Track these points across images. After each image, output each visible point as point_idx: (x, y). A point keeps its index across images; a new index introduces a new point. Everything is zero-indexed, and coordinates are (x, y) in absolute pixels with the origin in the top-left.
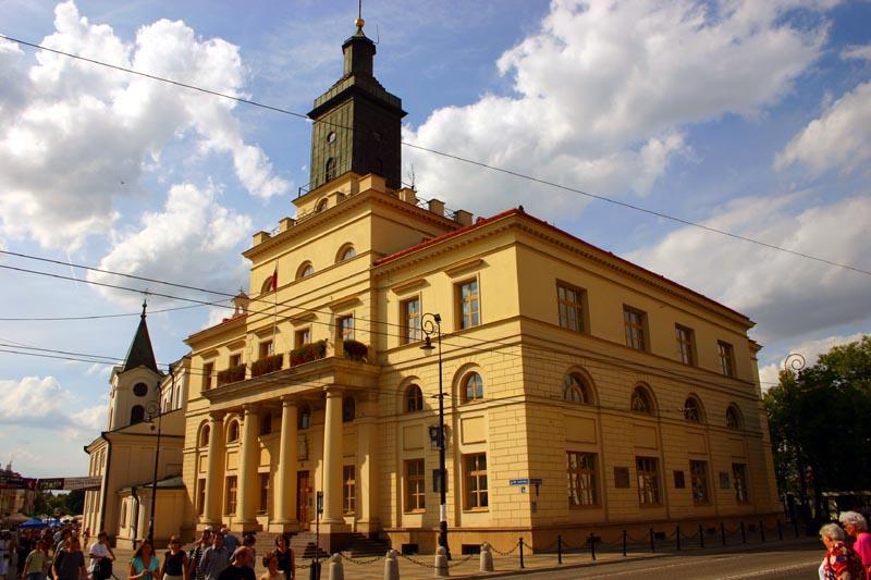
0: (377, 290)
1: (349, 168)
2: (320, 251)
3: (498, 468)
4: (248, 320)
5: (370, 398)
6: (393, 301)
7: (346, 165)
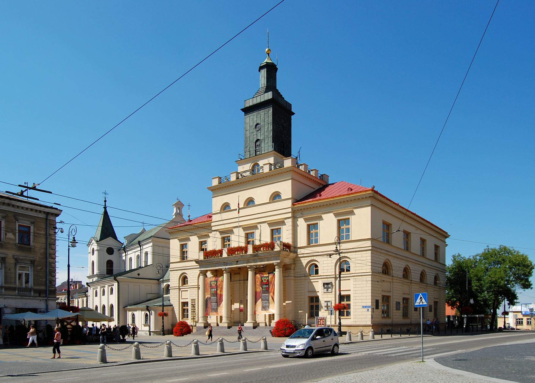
0: (294, 218)
1: (271, 149)
2: (261, 193)
3: (355, 301)
5: (292, 268)
6: (302, 224)
7: (268, 145)
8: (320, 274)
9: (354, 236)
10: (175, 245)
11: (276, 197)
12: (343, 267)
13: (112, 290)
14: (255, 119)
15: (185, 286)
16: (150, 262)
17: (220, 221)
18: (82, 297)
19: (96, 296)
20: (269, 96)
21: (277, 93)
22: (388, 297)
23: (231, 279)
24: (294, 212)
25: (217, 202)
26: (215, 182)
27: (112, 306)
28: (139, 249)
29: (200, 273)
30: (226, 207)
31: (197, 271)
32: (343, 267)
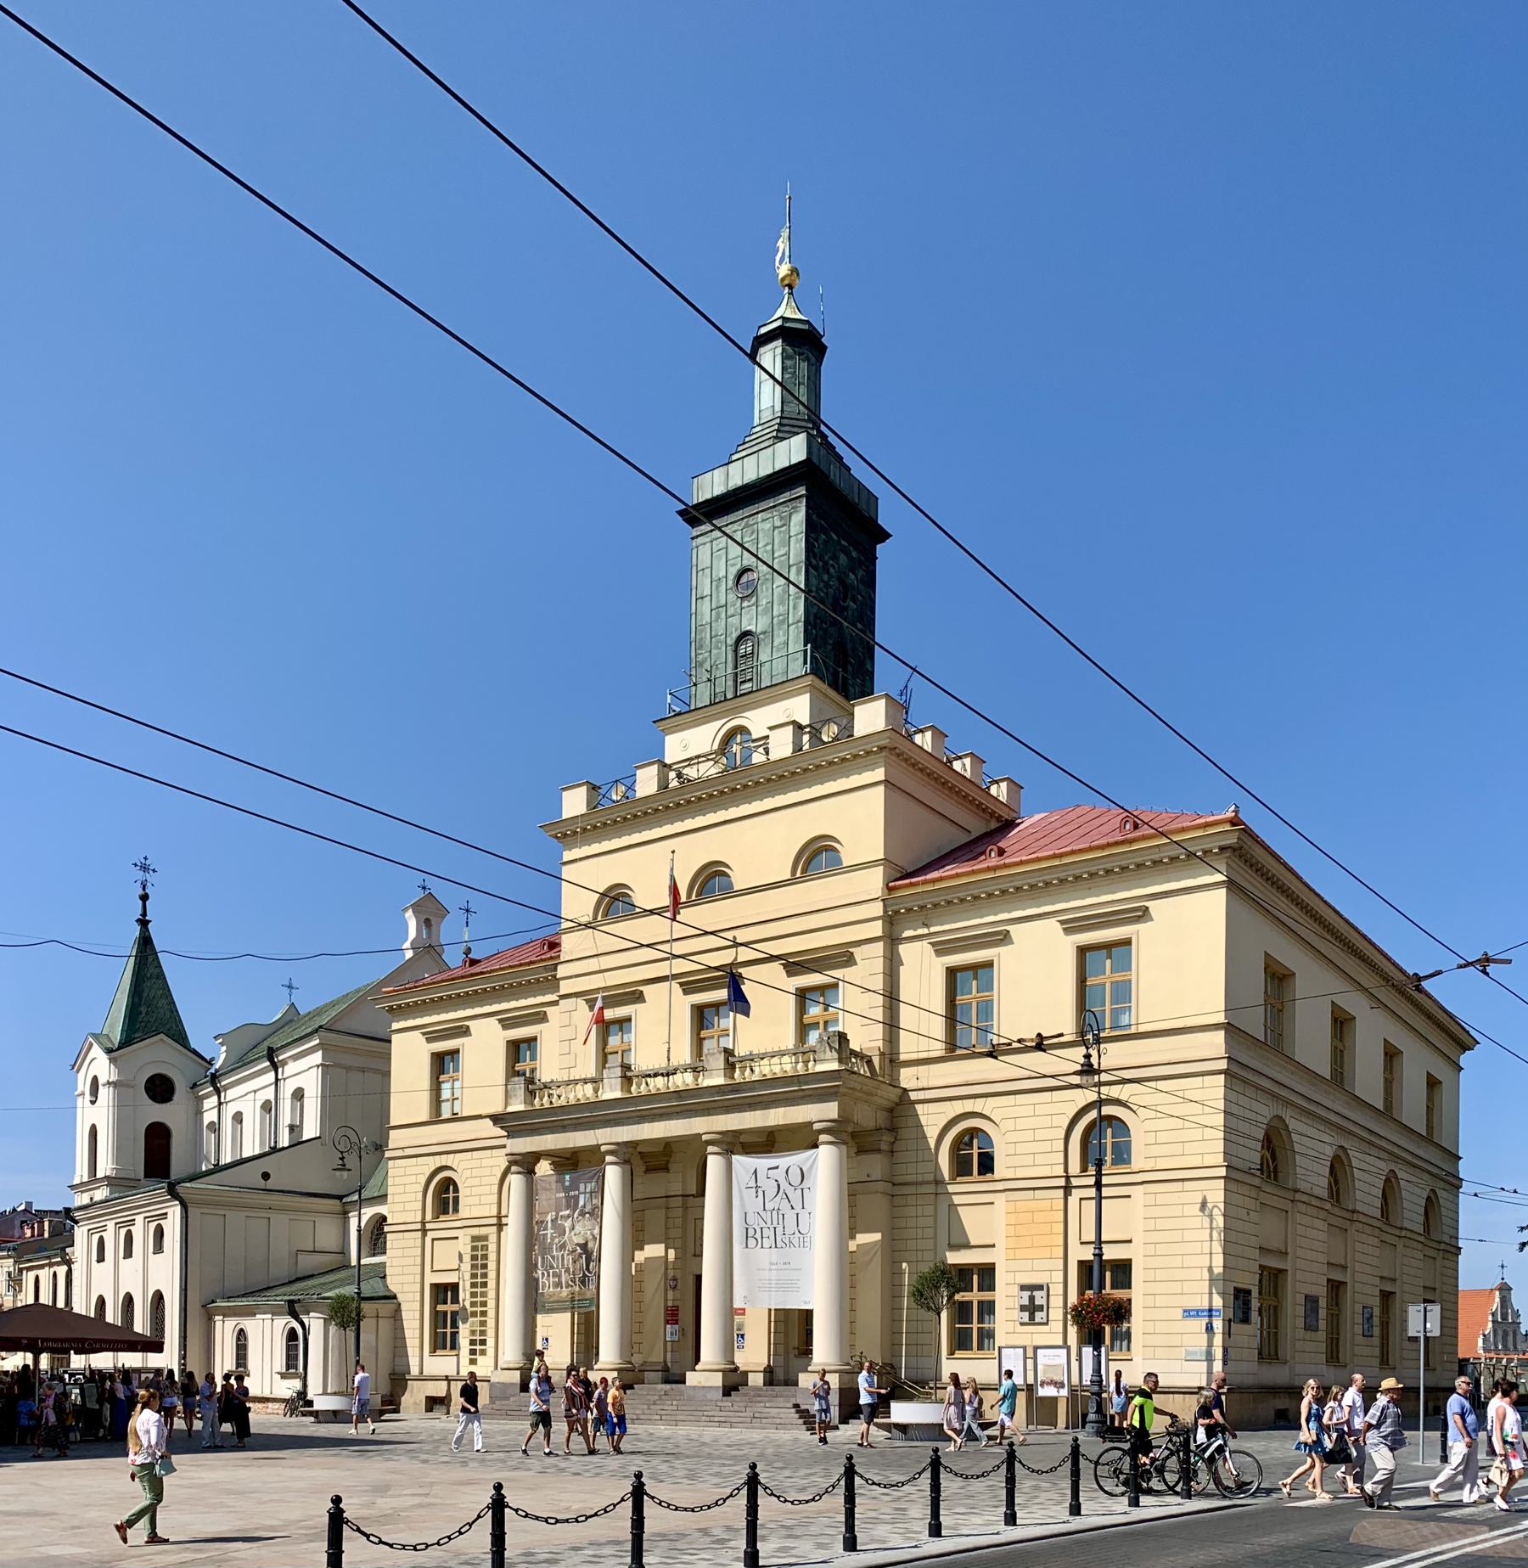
0: (892, 940)
1: (798, 667)
2: (757, 842)
3: (1152, 1288)
4: (562, 971)
7: (786, 649)
8: (998, 1174)
9: (1147, 1010)
10: (409, 1054)
12: (1100, 1143)
13: (159, 1233)
15: (447, 1221)
16: (311, 1130)
17: (587, 956)
18: (51, 1265)
19: (101, 1259)
20: (794, 450)
21: (820, 444)
22: (1279, 1273)
26: (574, 803)
27: (158, 1298)
28: (271, 1076)
29: (512, 1163)
30: (615, 902)
31: (499, 1161)
32: (1100, 1143)
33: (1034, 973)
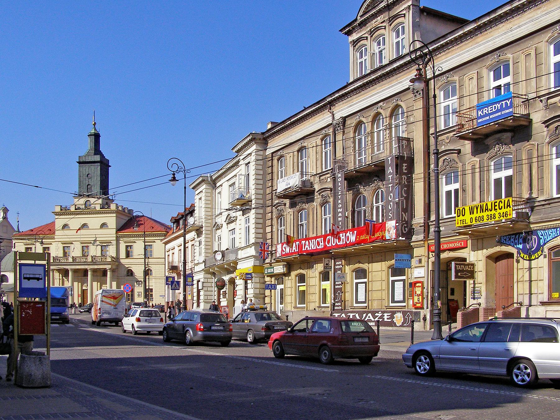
2: (94, 221)
11: (103, 225)
14: (87, 170)
21: (102, 156)
23: (93, 275)
24: (117, 237)
25: (60, 222)
26: (58, 209)
30: (65, 226)
33: (138, 247)
